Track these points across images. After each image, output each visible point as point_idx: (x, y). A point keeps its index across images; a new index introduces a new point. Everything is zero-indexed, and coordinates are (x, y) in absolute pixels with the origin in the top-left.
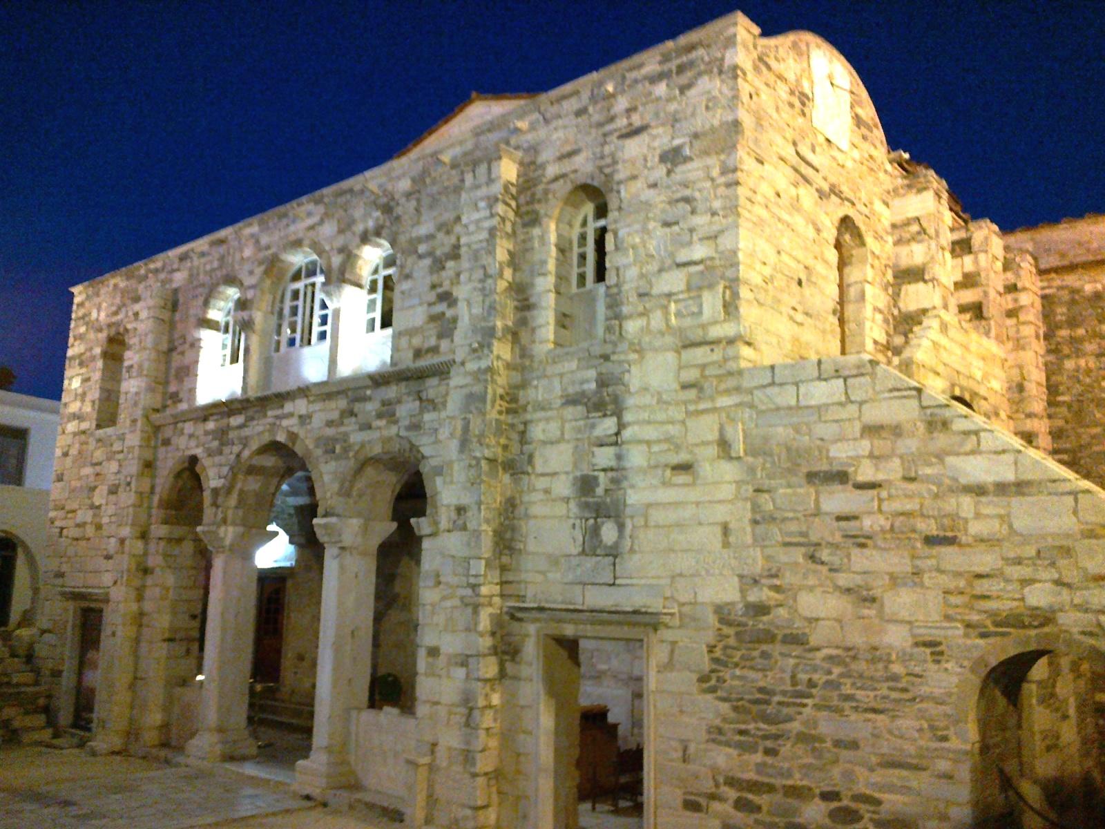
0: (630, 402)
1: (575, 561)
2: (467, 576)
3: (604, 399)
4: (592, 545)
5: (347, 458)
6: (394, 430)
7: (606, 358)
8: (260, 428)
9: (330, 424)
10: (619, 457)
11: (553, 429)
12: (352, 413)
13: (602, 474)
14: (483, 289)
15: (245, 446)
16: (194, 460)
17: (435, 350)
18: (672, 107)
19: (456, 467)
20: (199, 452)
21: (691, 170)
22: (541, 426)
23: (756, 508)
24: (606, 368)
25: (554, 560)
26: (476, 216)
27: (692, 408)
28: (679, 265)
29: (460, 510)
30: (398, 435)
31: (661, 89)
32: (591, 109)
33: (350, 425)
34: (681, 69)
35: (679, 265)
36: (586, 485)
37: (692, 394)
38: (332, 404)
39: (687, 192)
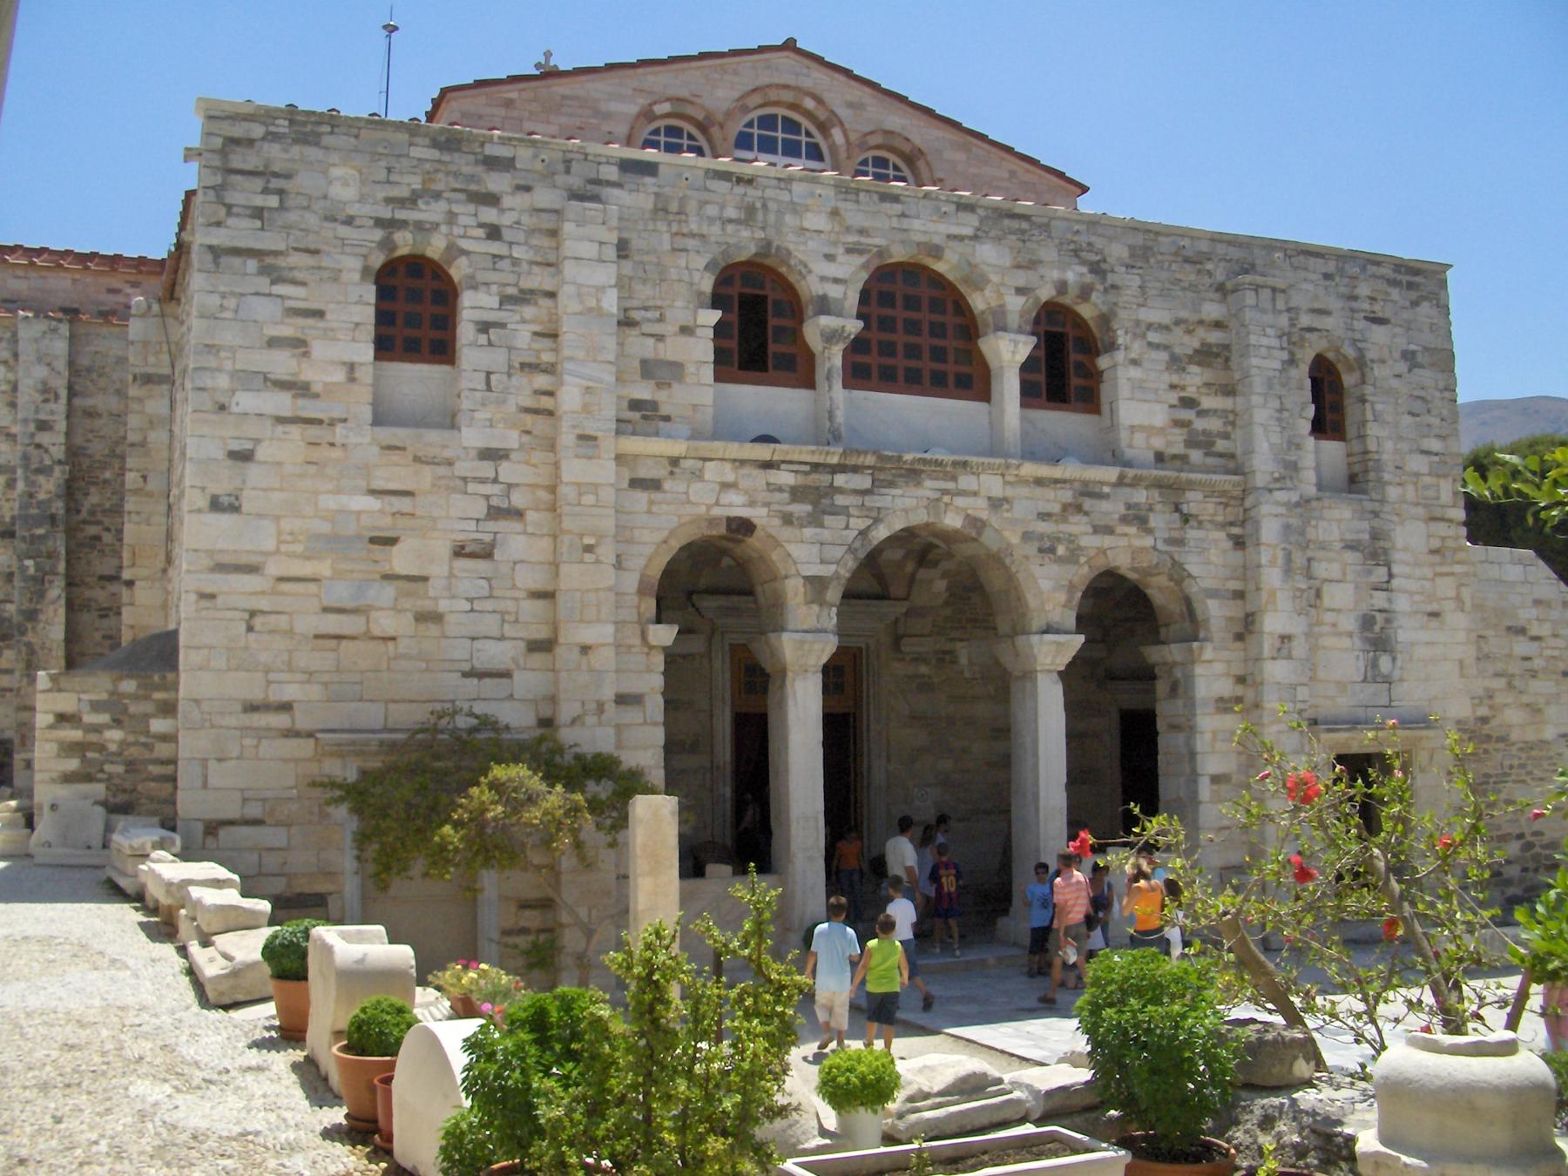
0: (1396, 556)
1: (1358, 687)
2: (1295, 702)
3: (1375, 550)
4: (1373, 675)
5: (1076, 562)
6: (1148, 542)
7: (1376, 514)
8: (910, 503)
9: (1044, 516)
10: (1390, 600)
11: (1334, 570)
12: (1079, 509)
13: (1378, 615)
14: (1279, 420)
15: (877, 521)
16: (743, 527)
17: (1183, 458)
18: (1406, 315)
19: (1279, 594)
20: (757, 514)
21: (1426, 376)
22: (1324, 565)
23: (1479, 649)
24: (1376, 523)
25: (1341, 686)
26: (1265, 341)
27: (1439, 569)
28: (1424, 452)
29: (1285, 638)
30: (1154, 548)
31: (1395, 294)
32: (1337, 279)
33: (1077, 526)
34: (1410, 286)
35: (1424, 452)
36: (1367, 622)
37: (1437, 559)
38: (1049, 493)
39: (1422, 393)
